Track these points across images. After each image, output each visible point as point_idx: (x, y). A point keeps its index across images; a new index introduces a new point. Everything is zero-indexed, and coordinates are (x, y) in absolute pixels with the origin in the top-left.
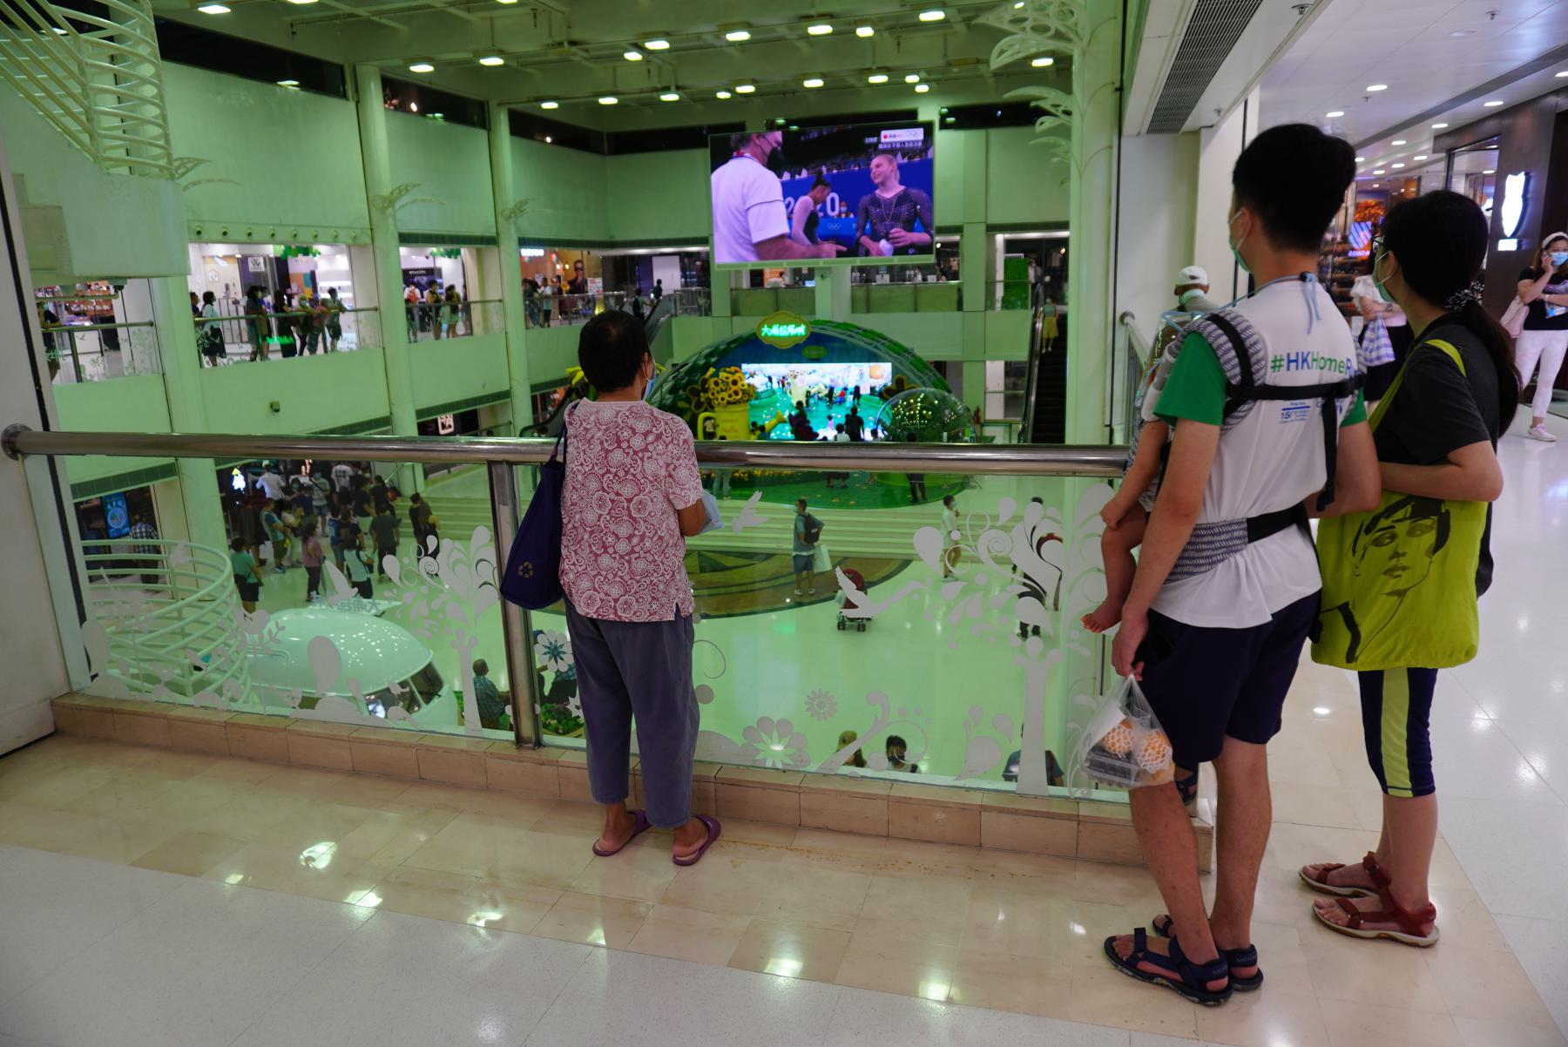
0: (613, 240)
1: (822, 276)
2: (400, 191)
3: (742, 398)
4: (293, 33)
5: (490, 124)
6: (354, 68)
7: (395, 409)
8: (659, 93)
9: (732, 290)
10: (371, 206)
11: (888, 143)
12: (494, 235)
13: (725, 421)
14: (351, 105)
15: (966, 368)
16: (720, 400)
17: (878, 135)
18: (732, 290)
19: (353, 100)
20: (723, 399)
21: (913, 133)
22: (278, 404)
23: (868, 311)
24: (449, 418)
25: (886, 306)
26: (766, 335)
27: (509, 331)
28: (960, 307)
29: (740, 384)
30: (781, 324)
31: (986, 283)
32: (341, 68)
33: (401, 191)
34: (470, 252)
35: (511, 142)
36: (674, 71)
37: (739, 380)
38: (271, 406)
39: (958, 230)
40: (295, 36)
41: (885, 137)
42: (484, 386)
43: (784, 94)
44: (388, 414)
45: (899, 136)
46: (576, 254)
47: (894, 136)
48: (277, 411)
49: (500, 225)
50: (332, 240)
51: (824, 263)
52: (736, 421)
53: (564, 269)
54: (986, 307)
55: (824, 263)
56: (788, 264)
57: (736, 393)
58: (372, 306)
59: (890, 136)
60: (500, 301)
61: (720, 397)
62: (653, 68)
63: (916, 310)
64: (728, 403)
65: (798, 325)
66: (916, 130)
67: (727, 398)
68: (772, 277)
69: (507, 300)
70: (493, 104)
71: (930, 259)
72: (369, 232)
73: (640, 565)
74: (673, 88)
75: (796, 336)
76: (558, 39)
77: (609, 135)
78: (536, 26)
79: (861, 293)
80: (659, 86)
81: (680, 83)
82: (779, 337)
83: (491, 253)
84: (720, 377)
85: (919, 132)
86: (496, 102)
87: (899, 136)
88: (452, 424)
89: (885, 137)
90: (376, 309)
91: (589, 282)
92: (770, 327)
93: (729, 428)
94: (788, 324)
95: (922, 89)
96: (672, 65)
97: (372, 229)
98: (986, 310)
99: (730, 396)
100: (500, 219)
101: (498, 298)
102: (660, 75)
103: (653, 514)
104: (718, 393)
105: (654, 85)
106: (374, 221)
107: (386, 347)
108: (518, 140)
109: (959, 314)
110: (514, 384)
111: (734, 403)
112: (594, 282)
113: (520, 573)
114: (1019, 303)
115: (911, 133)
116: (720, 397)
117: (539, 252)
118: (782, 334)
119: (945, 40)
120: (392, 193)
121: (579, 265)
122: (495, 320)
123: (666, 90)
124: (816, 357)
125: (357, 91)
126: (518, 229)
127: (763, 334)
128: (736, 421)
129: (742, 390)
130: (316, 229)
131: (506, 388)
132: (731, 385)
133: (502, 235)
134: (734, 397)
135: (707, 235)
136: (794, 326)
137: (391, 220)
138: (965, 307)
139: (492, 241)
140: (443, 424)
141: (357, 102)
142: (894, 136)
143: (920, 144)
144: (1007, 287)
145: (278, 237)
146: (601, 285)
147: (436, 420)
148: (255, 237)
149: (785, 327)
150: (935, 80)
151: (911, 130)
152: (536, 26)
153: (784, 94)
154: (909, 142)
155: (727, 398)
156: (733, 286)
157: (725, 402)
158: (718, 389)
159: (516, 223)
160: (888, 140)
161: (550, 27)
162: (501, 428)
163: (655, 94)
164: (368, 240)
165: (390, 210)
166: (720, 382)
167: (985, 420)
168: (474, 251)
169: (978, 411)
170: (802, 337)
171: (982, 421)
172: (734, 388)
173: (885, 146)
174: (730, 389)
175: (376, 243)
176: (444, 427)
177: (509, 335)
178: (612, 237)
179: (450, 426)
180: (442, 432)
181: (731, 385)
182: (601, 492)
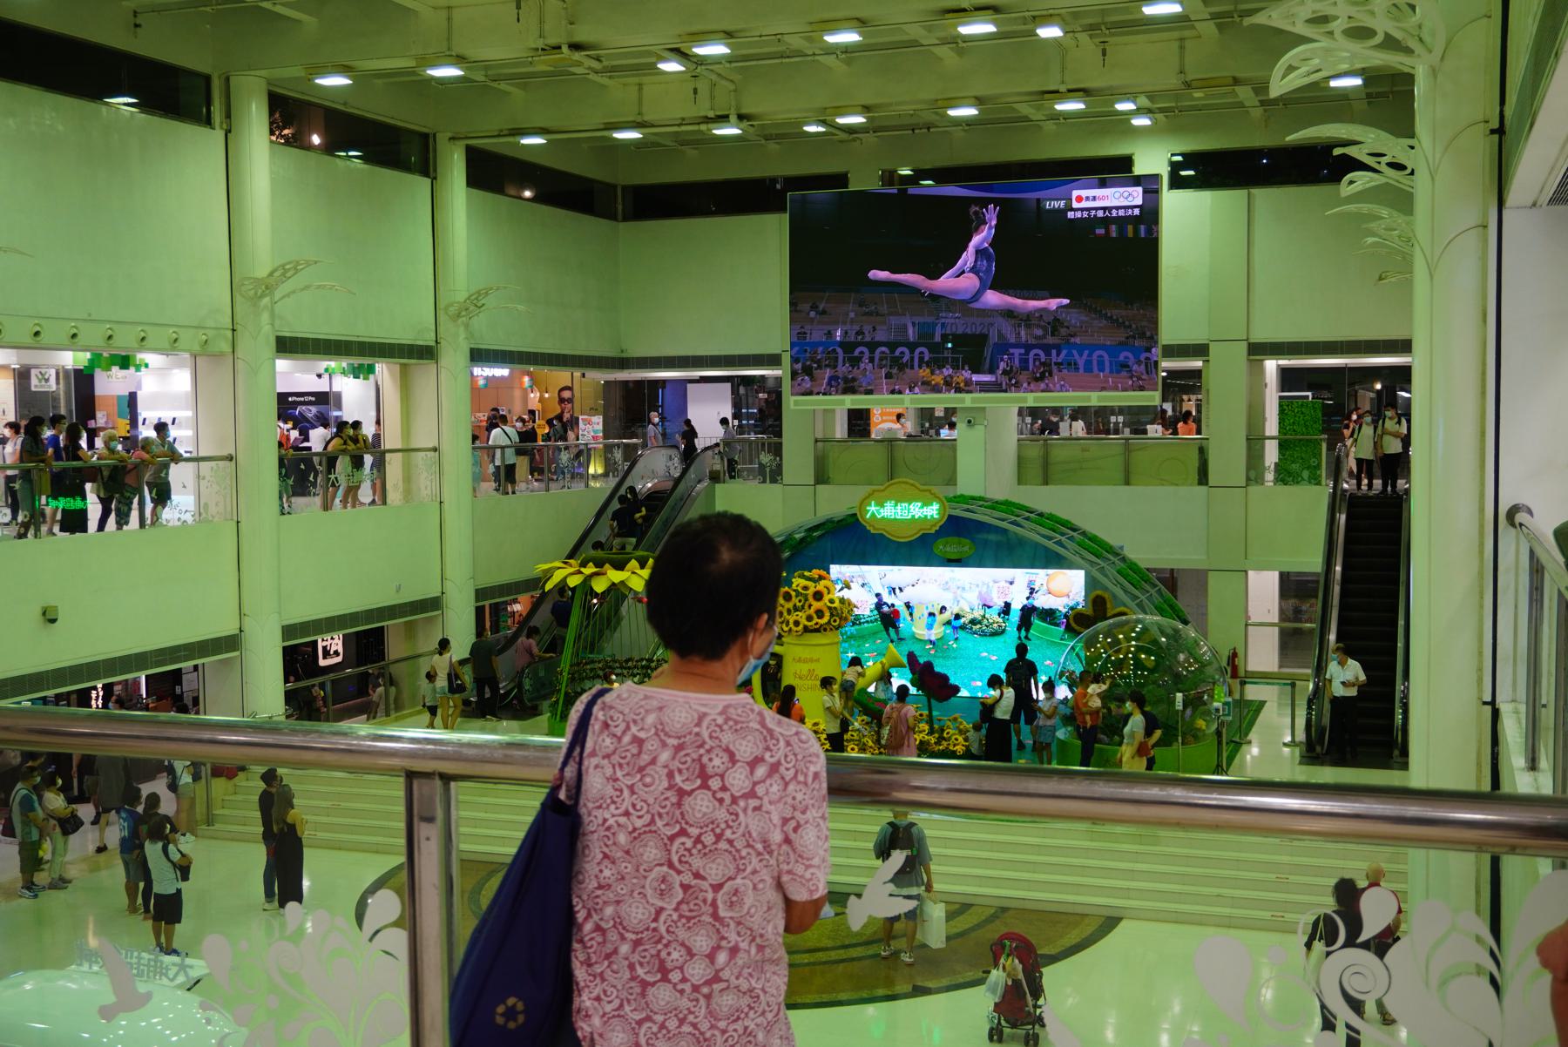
0: (624, 355)
1: (969, 422)
2: (286, 271)
3: (829, 621)
4: (137, 26)
5: (435, 171)
6: (227, 79)
7: (248, 624)
8: (710, 126)
9: (817, 441)
10: (238, 298)
11: (1082, 210)
12: (433, 344)
13: (800, 660)
14: (218, 135)
15: (1214, 581)
16: (791, 625)
18: (817, 441)
19: (221, 128)
20: (797, 623)
21: (1126, 194)
22: (55, 608)
23: (1046, 482)
24: (336, 641)
25: (1076, 474)
26: (873, 514)
27: (446, 498)
28: (1203, 477)
29: (826, 598)
30: (899, 500)
31: (1247, 439)
32: (207, 79)
33: (284, 272)
34: (390, 370)
35: (469, 198)
36: (735, 91)
37: (825, 591)
38: (44, 614)
39: (1201, 350)
40: (138, 29)
41: (1079, 199)
42: (398, 589)
44: (237, 632)
45: (1103, 198)
46: (562, 376)
47: (1094, 198)
48: (53, 621)
49: (441, 329)
50: (167, 345)
51: (973, 400)
52: (818, 660)
53: (541, 400)
54: (1248, 479)
55: (973, 400)
56: (912, 401)
57: (820, 613)
58: (225, 453)
59: (1087, 198)
60: (435, 450)
61: (792, 619)
62: (703, 87)
63: (1127, 483)
64: (806, 629)
65: (926, 504)
66: (1130, 189)
67: (804, 622)
68: (883, 421)
69: (445, 448)
70: (442, 139)
71: (1153, 399)
72: (229, 333)
73: (726, 1002)
74: (733, 119)
76: (552, 41)
77: (624, 188)
78: (518, 20)
79: (1034, 451)
80: (711, 114)
81: (744, 111)
82: (895, 519)
83: (424, 374)
84: (794, 586)
85: (1135, 194)
86: (450, 135)
87: (1103, 198)
88: (341, 650)
89: (1079, 199)
90: (230, 458)
91: (580, 421)
93: (805, 672)
94: (910, 501)
95: (1141, 121)
96: (732, 81)
97: (233, 330)
98: (1247, 485)
99: (809, 618)
100: (442, 317)
101: (431, 446)
102: (712, 97)
103: (753, 910)
104: (789, 611)
105: (703, 113)
106: (238, 318)
107: (243, 519)
108: (475, 192)
109: (1204, 488)
110: (448, 585)
111: (817, 631)
112: (589, 423)
113: (500, 1020)
114: (1306, 474)
115: (1122, 195)
116: (792, 619)
117: (502, 372)
119: (1182, 48)
120: (271, 274)
121: (566, 394)
122: (425, 484)
123: (723, 119)
124: (953, 557)
125: (228, 116)
126: (470, 336)
127: (868, 516)
128: (818, 660)
129: (830, 608)
130: (146, 328)
131: (435, 593)
132: (811, 600)
133: (443, 343)
134: (816, 620)
135: (777, 351)
136: (919, 504)
137: (265, 317)
138: (1212, 480)
139: (426, 353)
140: (324, 648)
141: (228, 132)
142: (1094, 198)
144: (1283, 446)
145: (80, 340)
146: (600, 427)
147: (316, 642)
148: (45, 338)
150: (1162, 110)
152: (518, 20)
153: (913, 130)
154: (1118, 208)
155: (804, 622)
156: (819, 435)
157: (801, 626)
158: (790, 605)
159: (467, 326)
160: (1084, 204)
161: (541, 22)
162: (421, 659)
163: (703, 127)
164: (227, 348)
165: (266, 300)
166: (793, 594)
167: (1246, 671)
168: (398, 367)
169: (1235, 655)
170: (935, 522)
171: (1241, 673)
172: (816, 605)
173: (1079, 215)
174: (810, 606)
175: (239, 354)
176: (326, 654)
177: (446, 506)
178: (622, 351)
179: (337, 653)
180: (322, 663)
181: (811, 600)
182: (665, 869)
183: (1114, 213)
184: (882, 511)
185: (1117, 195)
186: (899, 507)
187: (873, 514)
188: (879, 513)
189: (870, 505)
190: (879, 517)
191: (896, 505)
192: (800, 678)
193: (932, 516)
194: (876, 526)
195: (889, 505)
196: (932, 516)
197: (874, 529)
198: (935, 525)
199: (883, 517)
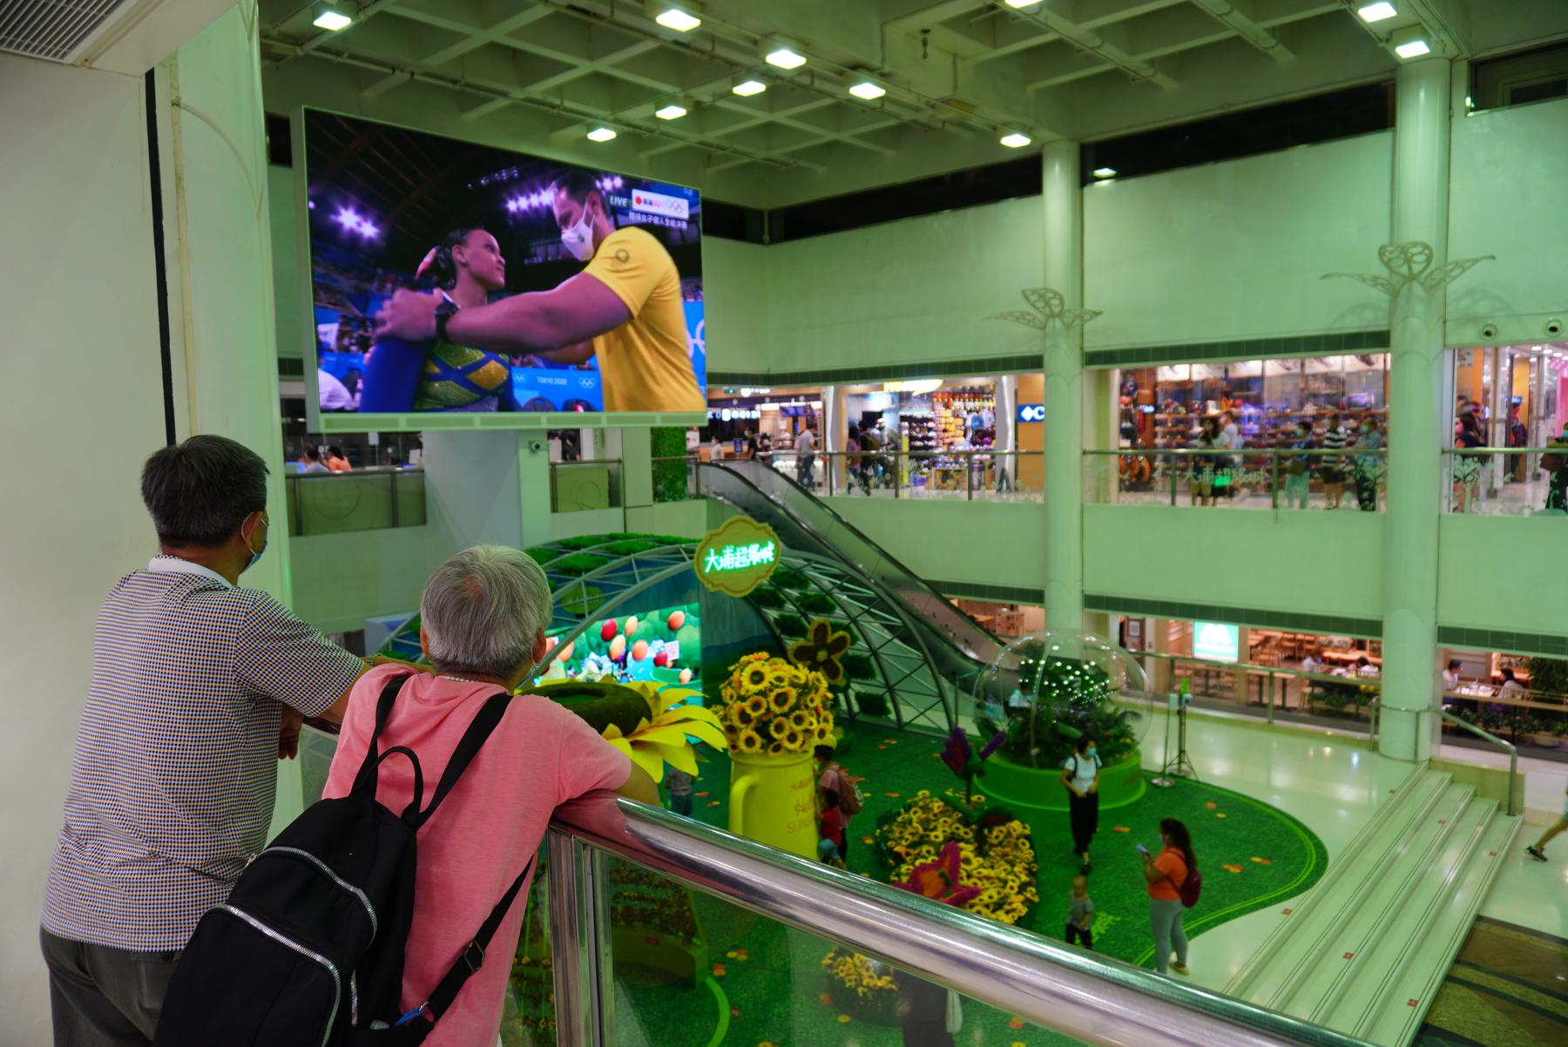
17: (629, 196)
26: (713, 567)
43: (394, 69)
45: (658, 204)
59: (645, 202)
75: (760, 565)
82: (734, 570)
85: (683, 206)
87: (658, 204)
92: (719, 553)
94: (747, 543)
118: (738, 566)
127: (707, 570)
136: (757, 546)
143: (684, 226)
149: (744, 549)
151: (673, 199)
183: (667, 223)
184: (721, 560)
185: (669, 204)
186: (738, 553)
187: (713, 567)
188: (719, 564)
189: (708, 554)
190: (719, 568)
191: (735, 550)
192: (804, 810)
193: (768, 561)
194: (715, 582)
195: (728, 550)
196: (768, 561)
197: (713, 586)
198: (768, 571)
199: (722, 570)
